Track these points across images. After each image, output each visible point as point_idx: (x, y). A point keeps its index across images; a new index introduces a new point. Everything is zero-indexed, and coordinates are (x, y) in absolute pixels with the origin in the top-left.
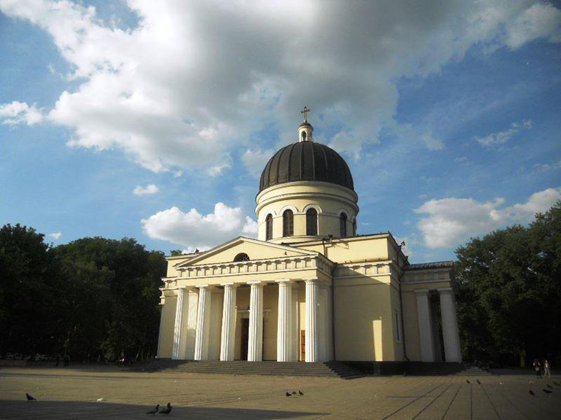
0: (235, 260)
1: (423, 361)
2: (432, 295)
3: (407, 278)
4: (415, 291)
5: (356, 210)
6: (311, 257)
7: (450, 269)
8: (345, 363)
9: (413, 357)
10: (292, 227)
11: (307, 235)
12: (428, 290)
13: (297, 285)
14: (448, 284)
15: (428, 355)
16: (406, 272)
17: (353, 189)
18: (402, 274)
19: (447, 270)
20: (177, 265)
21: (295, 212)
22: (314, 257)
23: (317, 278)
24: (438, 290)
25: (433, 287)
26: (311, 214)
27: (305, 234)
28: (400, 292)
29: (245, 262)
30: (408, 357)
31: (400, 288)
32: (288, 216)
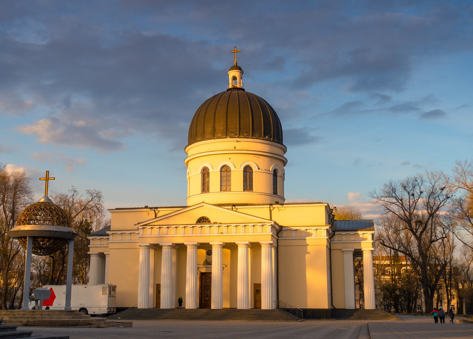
1: (346, 309)
4: (343, 250)
5: (284, 162)
8: (284, 309)
9: (338, 305)
11: (244, 190)
12: (353, 250)
15: (350, 304)
16: (336, 233)
17: (282, 144)
18: (334, 234)
20: (139, 223)
21: (232, 168)
22: (270, 224)
23: (272, 242)
26: (248, 171)
28: (330, 250)
30: (333, 305)
31: (330, 246)
32: (225, 170)
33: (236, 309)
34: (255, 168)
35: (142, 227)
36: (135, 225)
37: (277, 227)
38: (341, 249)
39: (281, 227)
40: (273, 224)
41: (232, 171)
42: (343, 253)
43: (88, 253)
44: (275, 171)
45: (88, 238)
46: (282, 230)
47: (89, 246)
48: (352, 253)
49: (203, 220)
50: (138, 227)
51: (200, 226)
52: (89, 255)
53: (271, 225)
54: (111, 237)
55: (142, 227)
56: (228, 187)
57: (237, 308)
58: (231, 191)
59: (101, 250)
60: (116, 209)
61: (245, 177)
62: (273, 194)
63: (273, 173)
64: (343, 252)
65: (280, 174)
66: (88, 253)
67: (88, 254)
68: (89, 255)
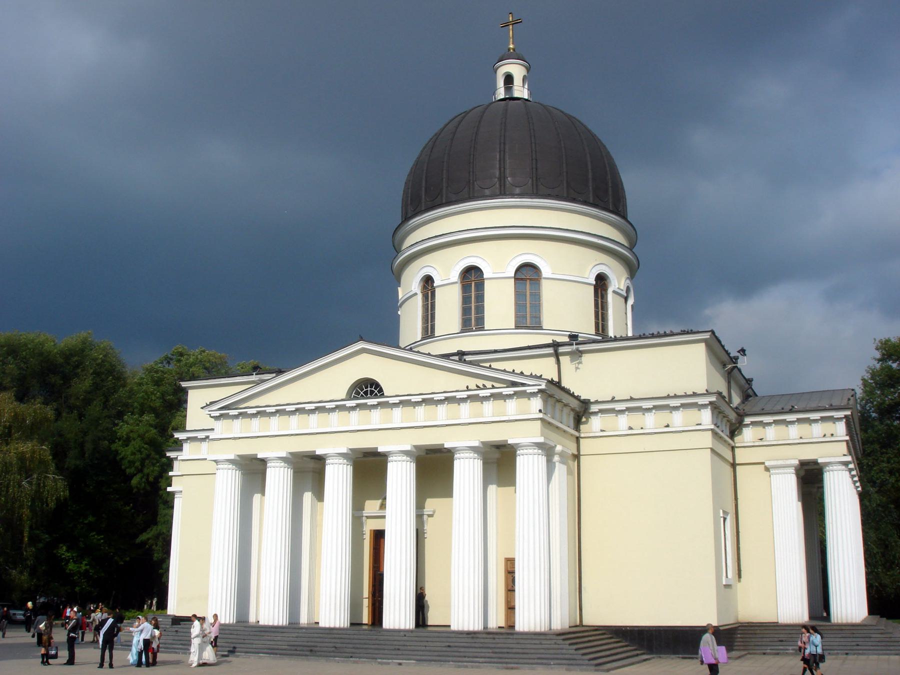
0: (349, 397)
2: (806, 471)
3: (748, 435)
4: (767, 464)
6: (529, 390)
7: (848, 413)
10: (480, 309)
12: (796, 462)
13: (496, 455)
14: (843, 448)
16: (748, 420)
17: (624, 217)
19: (841, 414)
20: (212, 403)
22: (535, 389)
24: (820, 461)
25: (808, 453)
27: (514, 328)
29: (374, 401)
34: (546, 271)
36: (202, 408)
37: (575, 404)
38: (763, 463)
39: (586, 403)
40: (543, 387)
42: (770, 471)
43: (169, 489)
44: (601, 281)
45: (168, 454)
47: (171, 474)
48: (792, 470)
49: (367, 387)
52: (172, 494)
53: (540, 391)
54: (186, 446)
55: (217, 414)
57: (449, 626)
58: (485, 329)
62: (594, 334)
63: (594, 283)
64: (767, 469)
65: (615, 286)
66: (169, 489)
67: (169, 492)
68: (172, 494)
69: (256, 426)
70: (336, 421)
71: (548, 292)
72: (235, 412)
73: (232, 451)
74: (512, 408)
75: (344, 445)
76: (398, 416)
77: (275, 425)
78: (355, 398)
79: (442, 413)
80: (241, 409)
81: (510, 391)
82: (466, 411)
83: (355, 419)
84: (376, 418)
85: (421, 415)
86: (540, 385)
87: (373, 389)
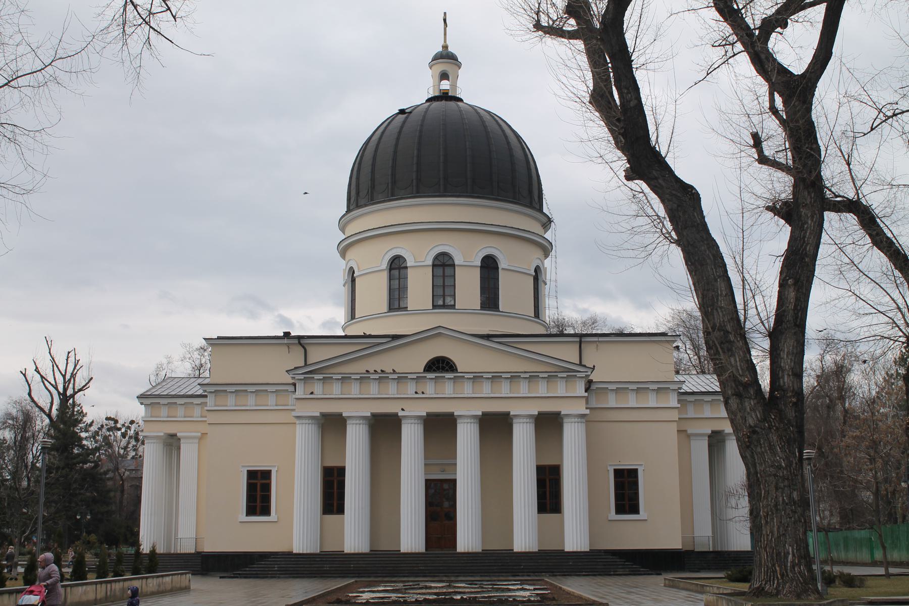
4: (689, 432)
20: (296, 368)
22: (583, 375)
33: (511, 551)
34: (502, 264)
35: (302, 377)
41: (458, 265)
46: (591, 388)
50: (294, 376)
51: (432, 375)
55: (302, 377)
56: (449, 301)
59: (171, 429)
60: (219, 338)
61: (483, 279)
69: (336, 390)
70: (410, 389)
71: (504, 279)
72: (321, 377)
73: (315, 410)
74: (560, 389)
75: (422, 410)
76: (467, 389)
77: (354, 390)
78: (434, 371)
79: (505, 389)
80: (325, 374)
81: (564, 375)
82: (523, 389)
83: (430, 389)
84: (448, 389)
85: (486, 389)
86: (587, 372)
87: (444, 365)
